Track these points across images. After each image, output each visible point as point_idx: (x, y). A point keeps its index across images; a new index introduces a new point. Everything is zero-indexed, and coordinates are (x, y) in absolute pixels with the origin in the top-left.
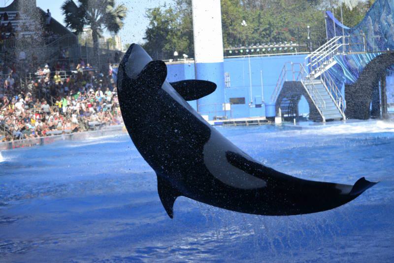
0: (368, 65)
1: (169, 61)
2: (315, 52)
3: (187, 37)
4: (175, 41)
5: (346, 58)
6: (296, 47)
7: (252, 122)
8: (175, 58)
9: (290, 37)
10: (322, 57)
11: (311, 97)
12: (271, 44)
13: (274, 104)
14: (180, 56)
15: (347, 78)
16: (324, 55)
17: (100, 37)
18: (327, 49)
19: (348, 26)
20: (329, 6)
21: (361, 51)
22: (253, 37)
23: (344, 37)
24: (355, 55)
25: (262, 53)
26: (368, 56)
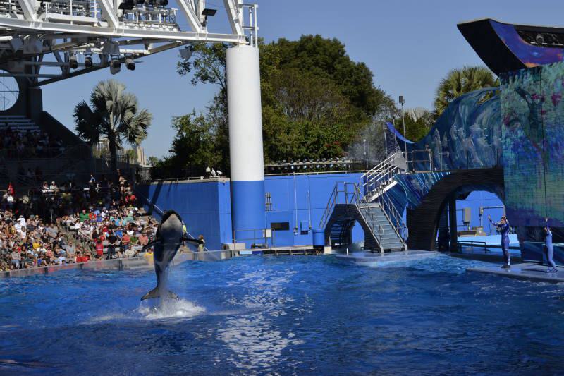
0: (435, 188)
3: (221, 151)
4: (208, 155)
6: (350, 164)
7: (297, 251)
10: (380, 176)
12: (321, 161)
16: (383, 174)
17: (119, 148)
19: (411, 140)
20: (390, 117)
21: (427, 170)
24: (419, 174)
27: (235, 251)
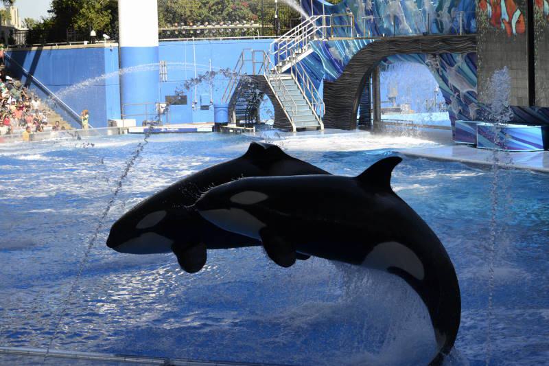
0: (356, 58)
1: (83, 44)
2: (284, 36)
3: (109, 11)
4: (92, 15)
5: (327, 46)
6: (259, 28)
8: (91, 40)
9: (251, 14)
10: (294, 42)
11: (277, 97)
12: (224, 24)
13: (227, 106)
14: (99, 36)
15: (327, 73)
16: (297, 41)
18: (301, 32)
21: (346, 37)
22: (200, 14)
23: (324, 16)
24: (339, 41)
25: (211, 35)
26: (356, 44)
27: (123, 128)
